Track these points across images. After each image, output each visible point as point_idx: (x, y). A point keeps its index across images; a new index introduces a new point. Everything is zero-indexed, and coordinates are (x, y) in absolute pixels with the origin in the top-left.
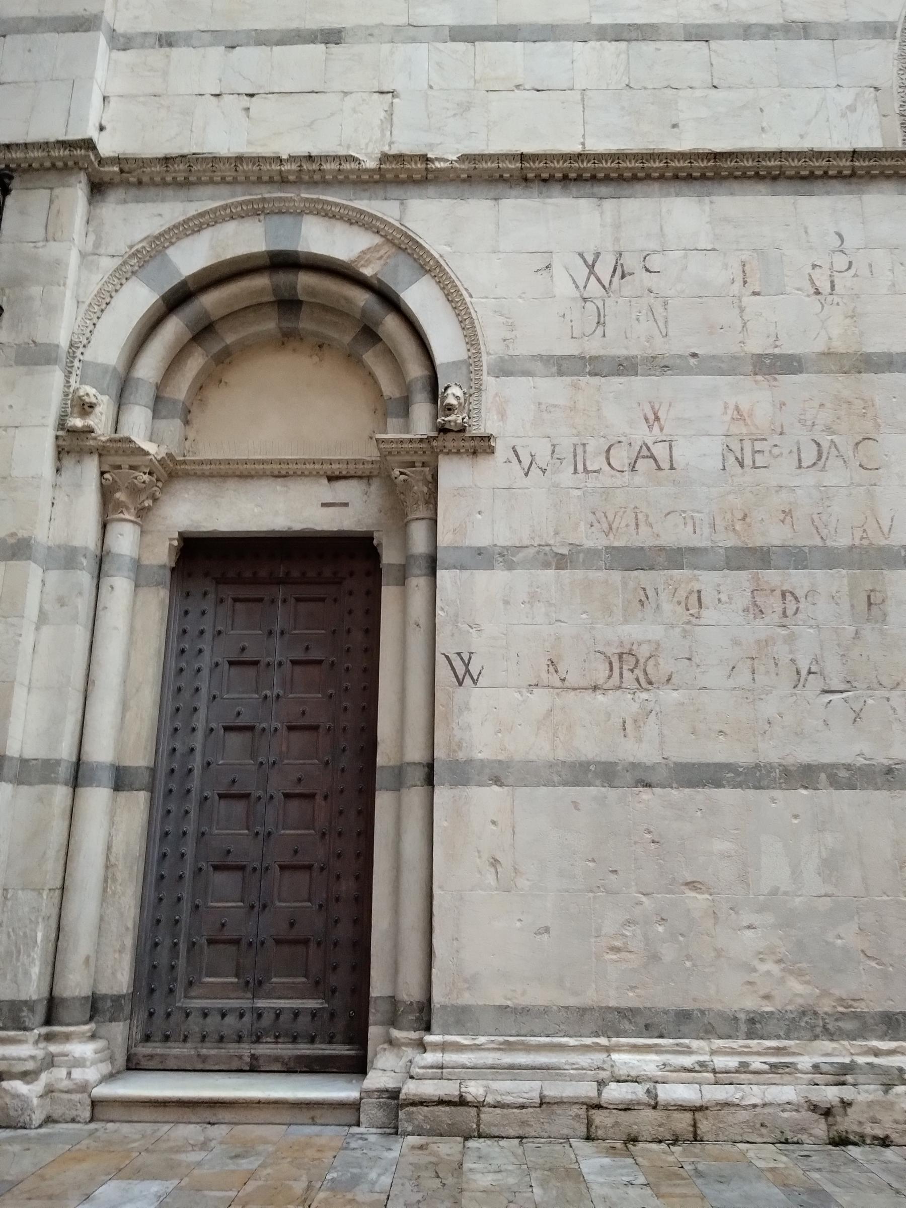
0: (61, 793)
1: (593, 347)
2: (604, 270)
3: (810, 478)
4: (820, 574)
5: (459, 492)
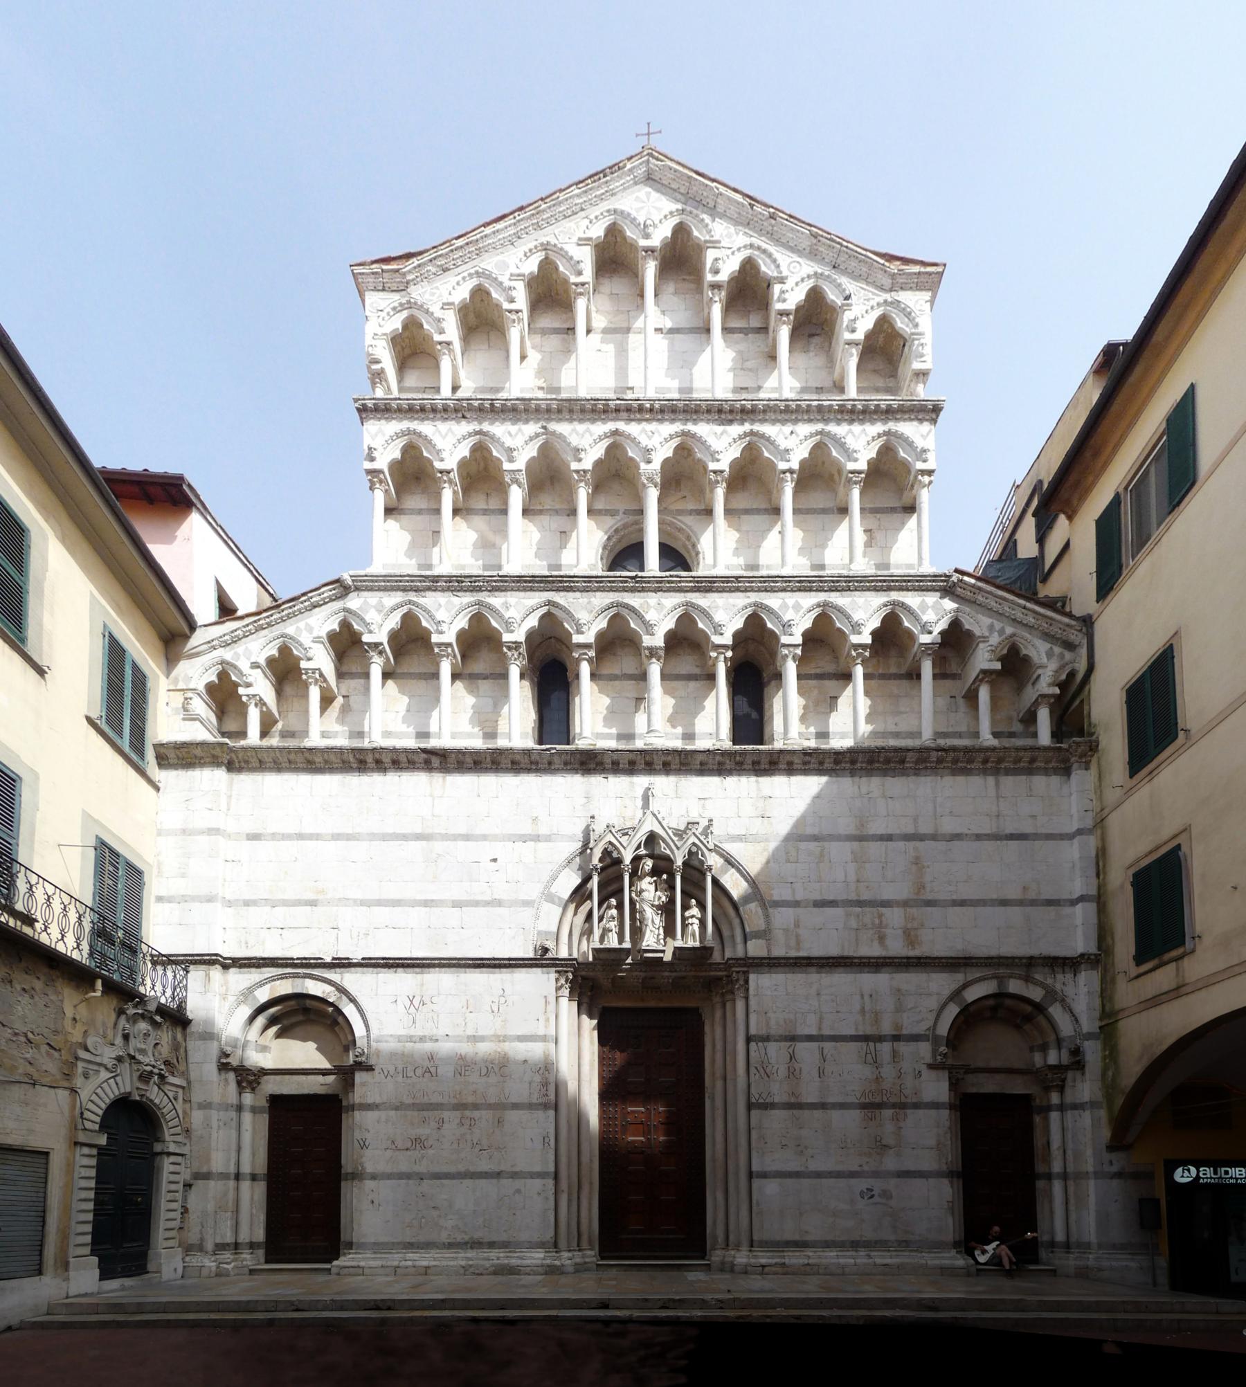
0: (232, 1183)
1: (412, 1032)
2: (416, 1002)
3: (484, 1080)
4: (484, 1112)
5: (363, 1084)
